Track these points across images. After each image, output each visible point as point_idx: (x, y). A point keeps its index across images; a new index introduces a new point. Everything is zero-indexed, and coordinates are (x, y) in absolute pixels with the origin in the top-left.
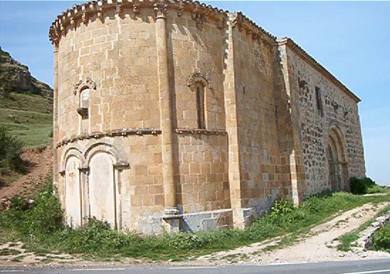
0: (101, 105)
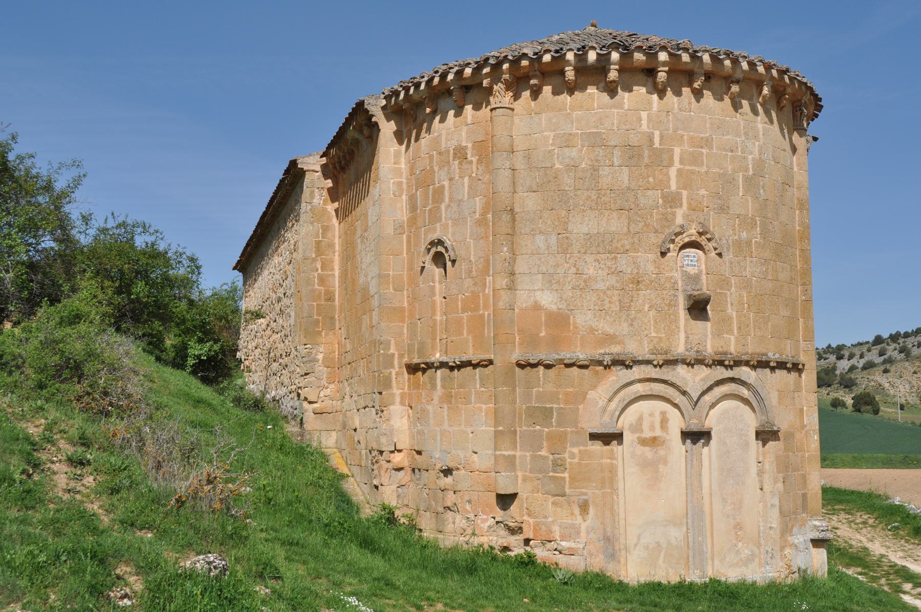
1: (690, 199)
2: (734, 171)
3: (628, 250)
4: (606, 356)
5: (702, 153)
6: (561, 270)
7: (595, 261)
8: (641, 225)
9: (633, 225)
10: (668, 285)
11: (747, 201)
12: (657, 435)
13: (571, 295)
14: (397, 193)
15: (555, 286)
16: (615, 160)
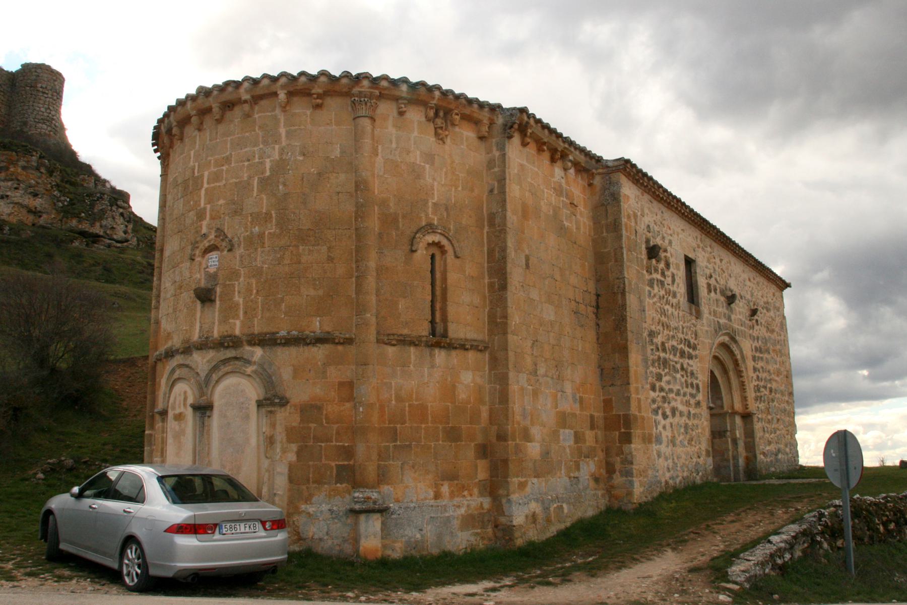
0: (240, 284)
1: (212, 210)
2: (250, 177)
5: (223, 170)
8: (185, 240)
9: (182, 242)
11: (261, 199)
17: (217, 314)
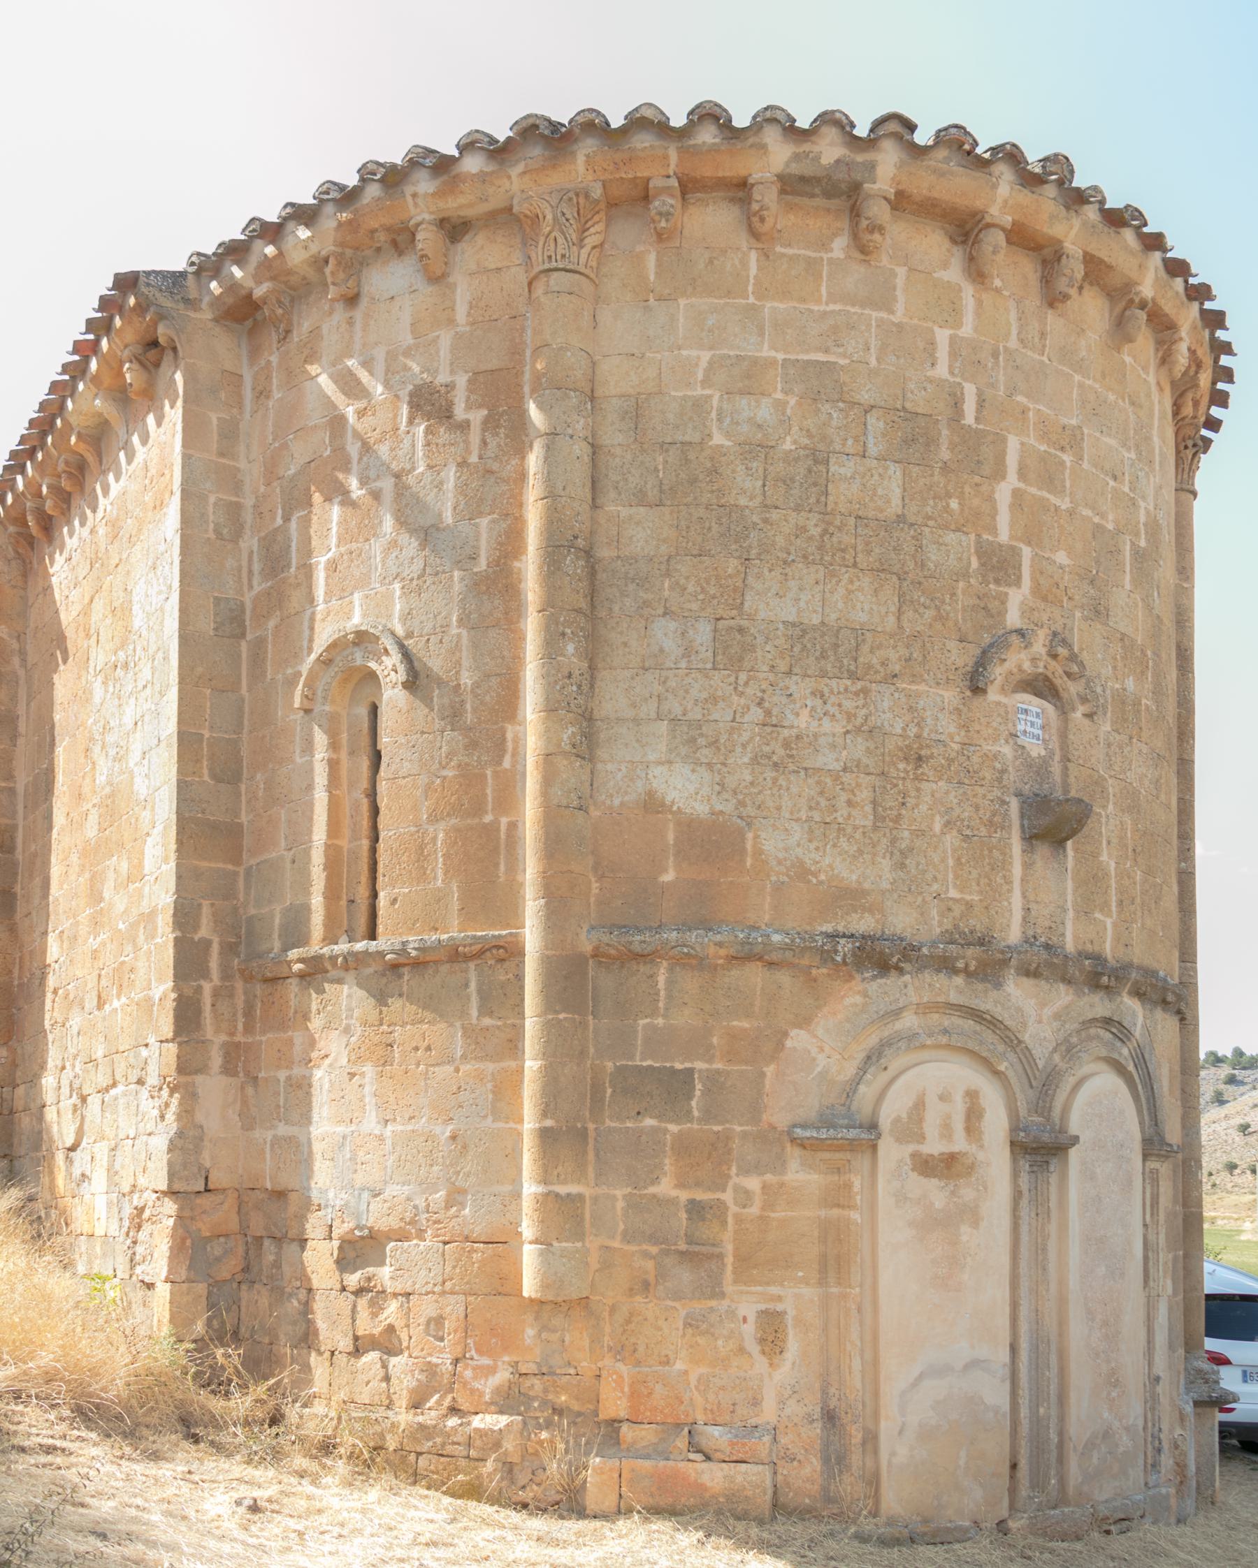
3: (895, 676)
4: (843, 941)
6: (721, 714)
7: (813, 693)
9: (909, 614)
10: (988, 774)
12: (956, 1148)
13: (749, 778)
14: (225, 531)
15: (705, 754)
16: (870, 445)
17: (1070, 884)
